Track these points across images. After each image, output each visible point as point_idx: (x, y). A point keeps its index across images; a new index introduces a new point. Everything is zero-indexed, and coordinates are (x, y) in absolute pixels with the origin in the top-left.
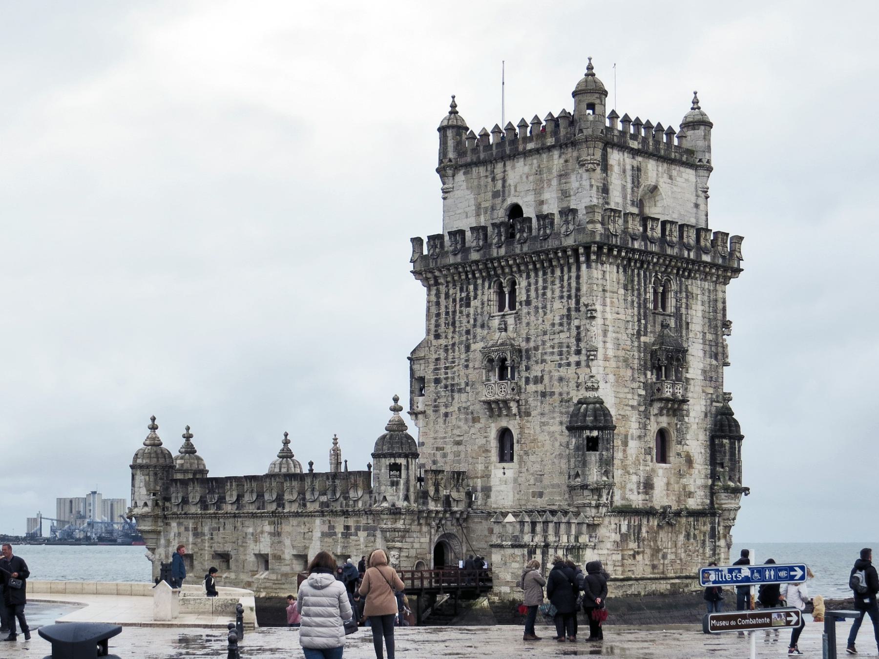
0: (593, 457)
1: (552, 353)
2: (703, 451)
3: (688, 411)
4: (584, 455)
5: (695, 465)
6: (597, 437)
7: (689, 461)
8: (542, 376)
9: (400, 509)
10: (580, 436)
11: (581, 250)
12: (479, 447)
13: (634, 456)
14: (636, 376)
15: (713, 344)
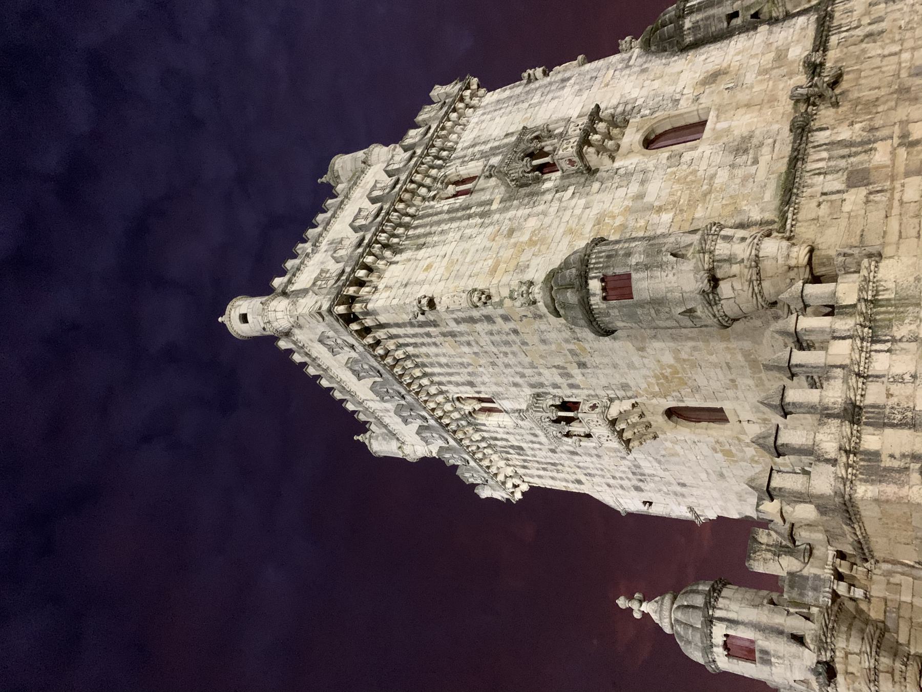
0: (644, 285)
1: (514, 354)
2: (704, 57)
3: (626, 104)
4: (641, 304)
5: (725, 65)
6: (602, 280)
7: (714, 77)
8: (554, 366)
9: (818, 662)
10: (608, 315)
11: (355, 326)
12: (715, 450)
13: (676, 187)
14: (541, 208)
15: (548, 89)
